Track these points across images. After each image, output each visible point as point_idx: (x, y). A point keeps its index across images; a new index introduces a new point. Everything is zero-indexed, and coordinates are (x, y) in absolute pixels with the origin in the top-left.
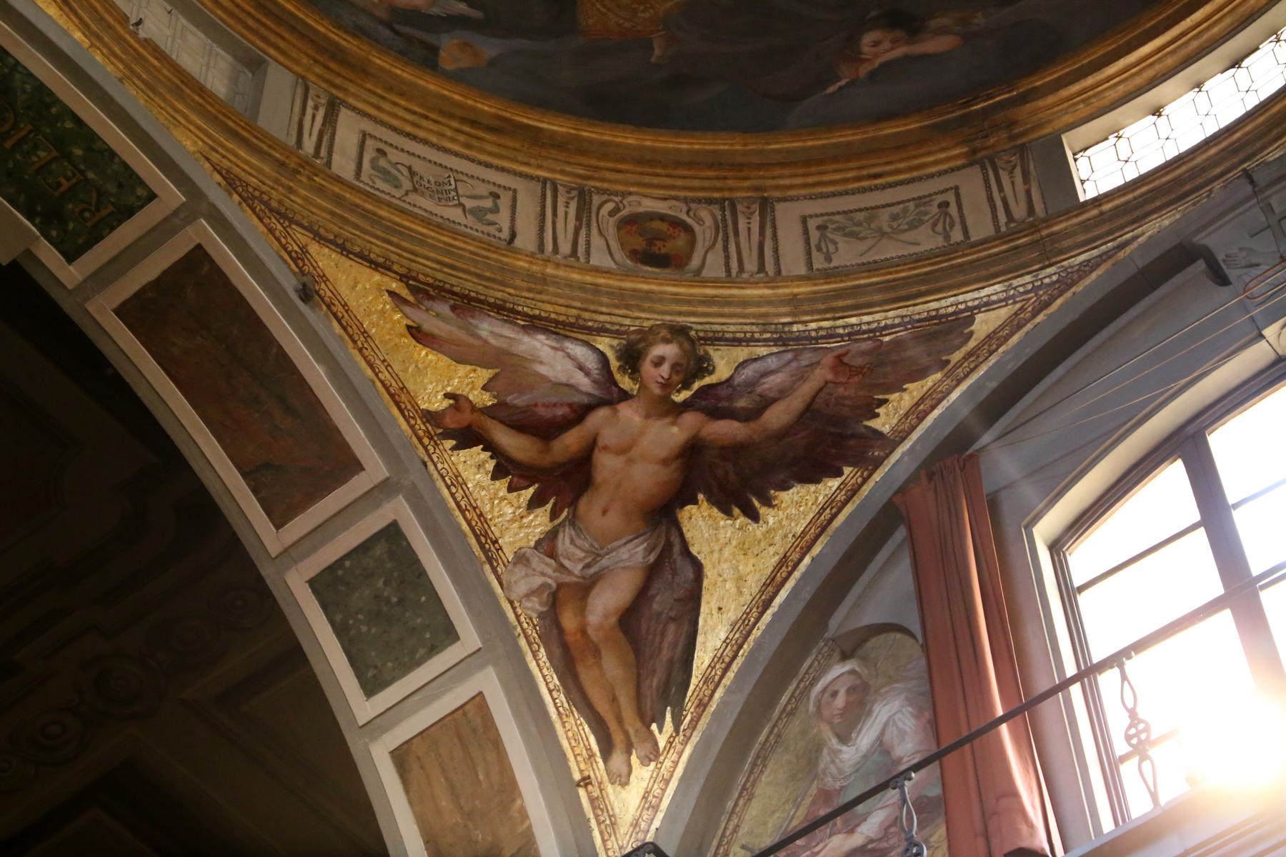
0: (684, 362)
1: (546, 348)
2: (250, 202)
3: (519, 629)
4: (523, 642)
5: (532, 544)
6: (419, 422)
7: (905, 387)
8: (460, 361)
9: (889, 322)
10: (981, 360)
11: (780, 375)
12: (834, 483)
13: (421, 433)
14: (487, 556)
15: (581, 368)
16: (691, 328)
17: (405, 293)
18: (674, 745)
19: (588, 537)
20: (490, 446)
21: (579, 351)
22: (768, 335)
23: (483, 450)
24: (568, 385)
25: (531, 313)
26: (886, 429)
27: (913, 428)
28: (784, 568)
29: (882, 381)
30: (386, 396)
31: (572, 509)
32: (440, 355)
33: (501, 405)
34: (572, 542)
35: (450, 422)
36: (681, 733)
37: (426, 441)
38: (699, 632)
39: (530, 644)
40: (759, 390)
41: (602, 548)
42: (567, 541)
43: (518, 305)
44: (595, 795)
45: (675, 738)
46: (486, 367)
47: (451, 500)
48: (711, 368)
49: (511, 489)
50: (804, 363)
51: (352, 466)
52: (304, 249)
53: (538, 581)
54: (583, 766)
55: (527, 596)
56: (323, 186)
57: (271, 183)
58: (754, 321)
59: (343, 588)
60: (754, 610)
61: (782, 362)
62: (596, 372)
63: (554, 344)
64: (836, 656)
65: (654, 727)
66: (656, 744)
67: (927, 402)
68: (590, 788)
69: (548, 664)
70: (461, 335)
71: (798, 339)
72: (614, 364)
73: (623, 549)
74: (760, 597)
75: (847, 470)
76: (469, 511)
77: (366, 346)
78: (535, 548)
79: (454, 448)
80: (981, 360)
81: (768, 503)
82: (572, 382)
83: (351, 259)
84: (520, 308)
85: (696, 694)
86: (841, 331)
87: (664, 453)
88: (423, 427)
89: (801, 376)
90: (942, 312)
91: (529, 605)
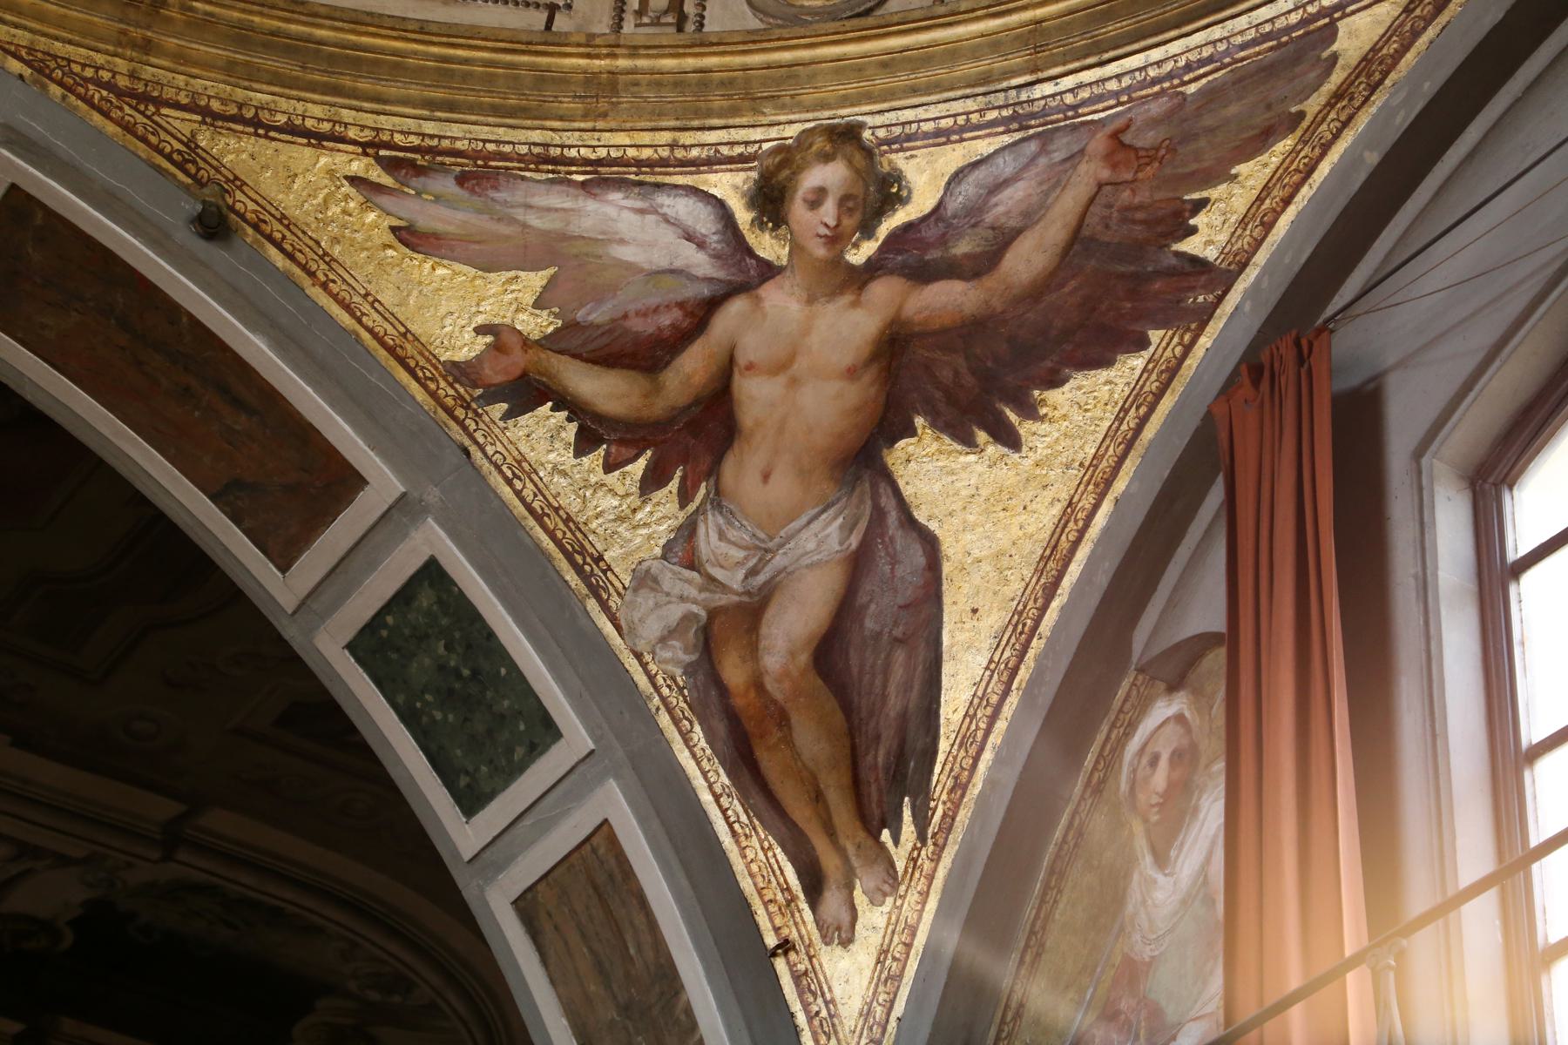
0: (859, 190)
1: (626, 215)
2: (81, 90)
3: (656, 700)
4: (664, 720)
5: (658, 551)
6: (443, 384)
7: (1233, 171)
8: (489, 266)
9: (1193, 56)
10: (1357, 103)
11: (1021, 185)
12: (1138, 362)
13: (450, 402)
14: (589, 586)
15: (689, 237)
16: (862, 126)
17: (377, 175)
18: (920, 862)
19: (745, 522)
20: (565, 402)
21: (681, 207)
22: (992, 115)
23: (552, 410)
24: (672, 272)
25: (593, 157)
26: (1211, 254)
27: (1258, 243)
28: (1071, 525)
29: (1194, 166)
30: (382, 353)
31: (712, 481)
32: (458, 267)
33: (570, 327)
34: (722, 536)
35: (495, 374)
36: (930, 842)
37: (460, 413)
38: (945, 657)
39: (676, 722)
40: (989, 218)
41: (771, 539)
42: (714, 536)
43: (570, 147)
44: (801, 967)
46: (535, 267)
47: (517, 502)
48: (904, 193)
49: (609, 467)
50: (1058, 156)
51: (347, 482)
52: (191, 143)
53: (676, 612)
54: (778, 921)
55: (663, 640)
56: (211, 14)
57: (111, 48)
58: (968, 91)
59: (394, 656)
60: (1031, 604)
61: (1024, 160)
62: (715, 238)
63: (639, 204)
64: (1162, 686)
65: (886, 835)
66: (892, 865)
67: (1275, 192)
68: (792, 956)
69: (709, 752)
70: (482, 223)
71: (1044, 113)
72: (743, 216)
73: (804, 535)
74: (1038, 580)
75: (1155, 336)
76: (548, 516)
77: (332, 276)
78: (664, 557)
79: (506, 416)
80: (1357, 103)
81: (1030, 411)
82: (678, 264)
83: (274, 139)
84: (573, 153)
85: (948, 768)
86: (1113, 86)
87: (846, 358)
88: (451, 392)
89: (1056, 182)
90: (1280, 23)
91: (668, 655)
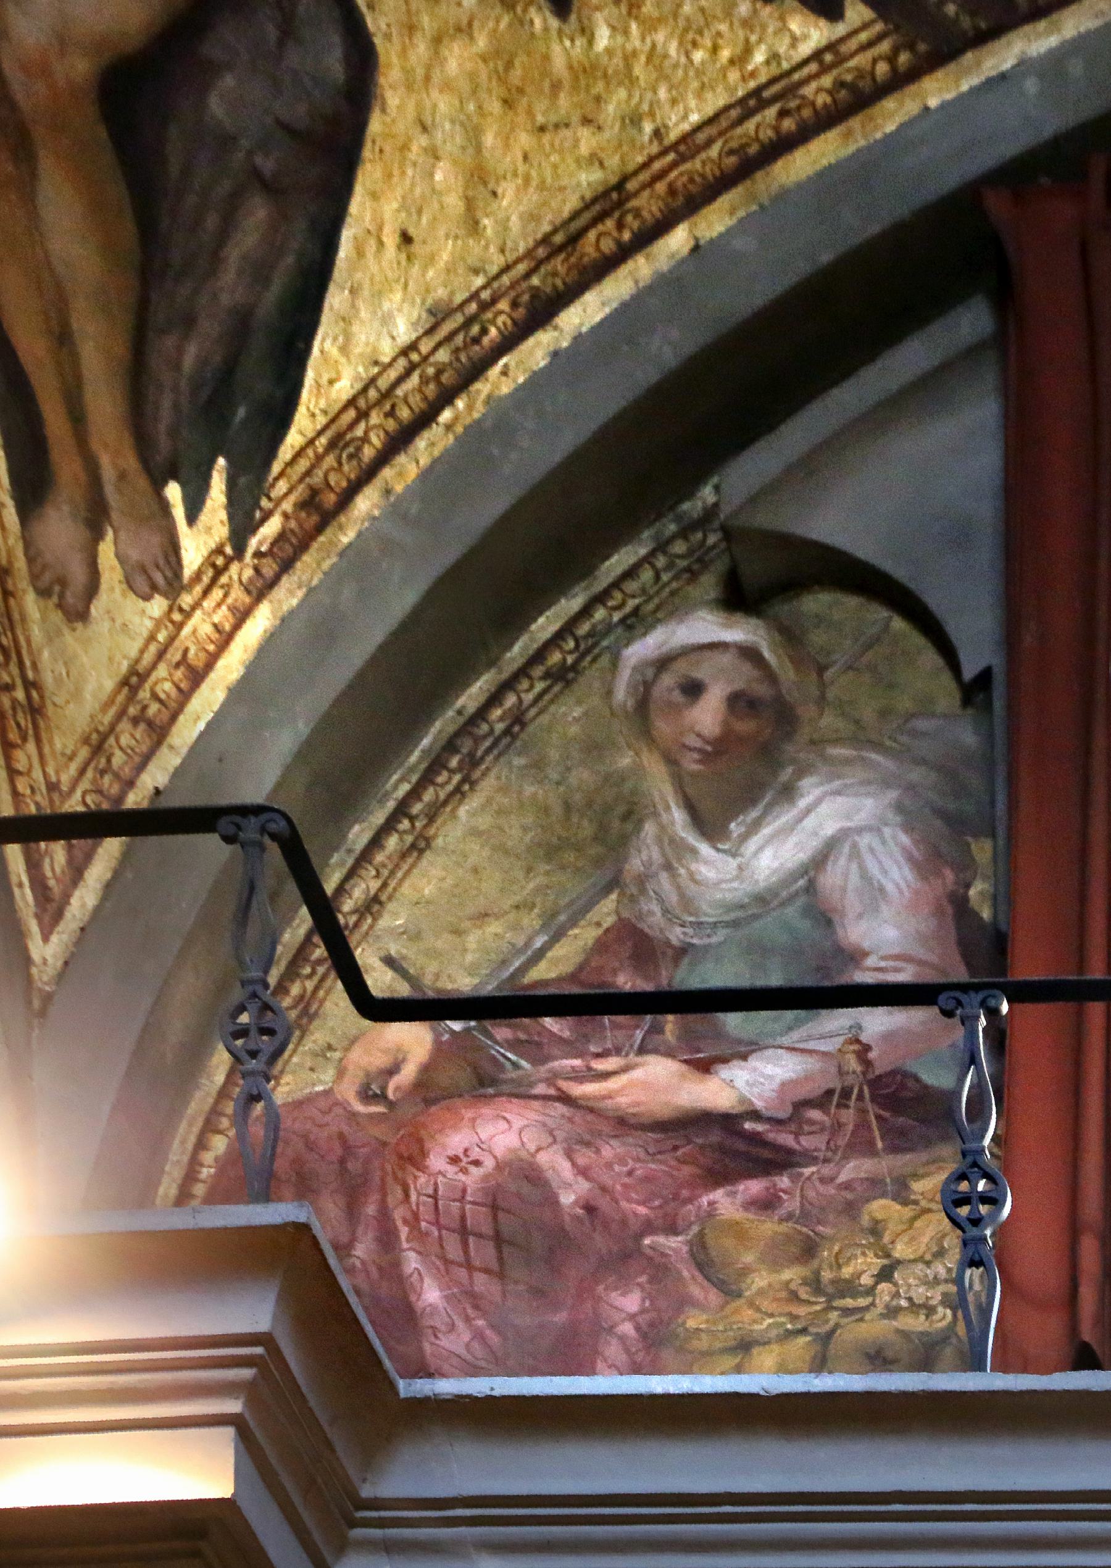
28: (610, 224)
45: (229, 561)
60: (503, 305)
65: (173, 492)
66: (173, 548)
74: (528, 275)
85: (303, 464)
